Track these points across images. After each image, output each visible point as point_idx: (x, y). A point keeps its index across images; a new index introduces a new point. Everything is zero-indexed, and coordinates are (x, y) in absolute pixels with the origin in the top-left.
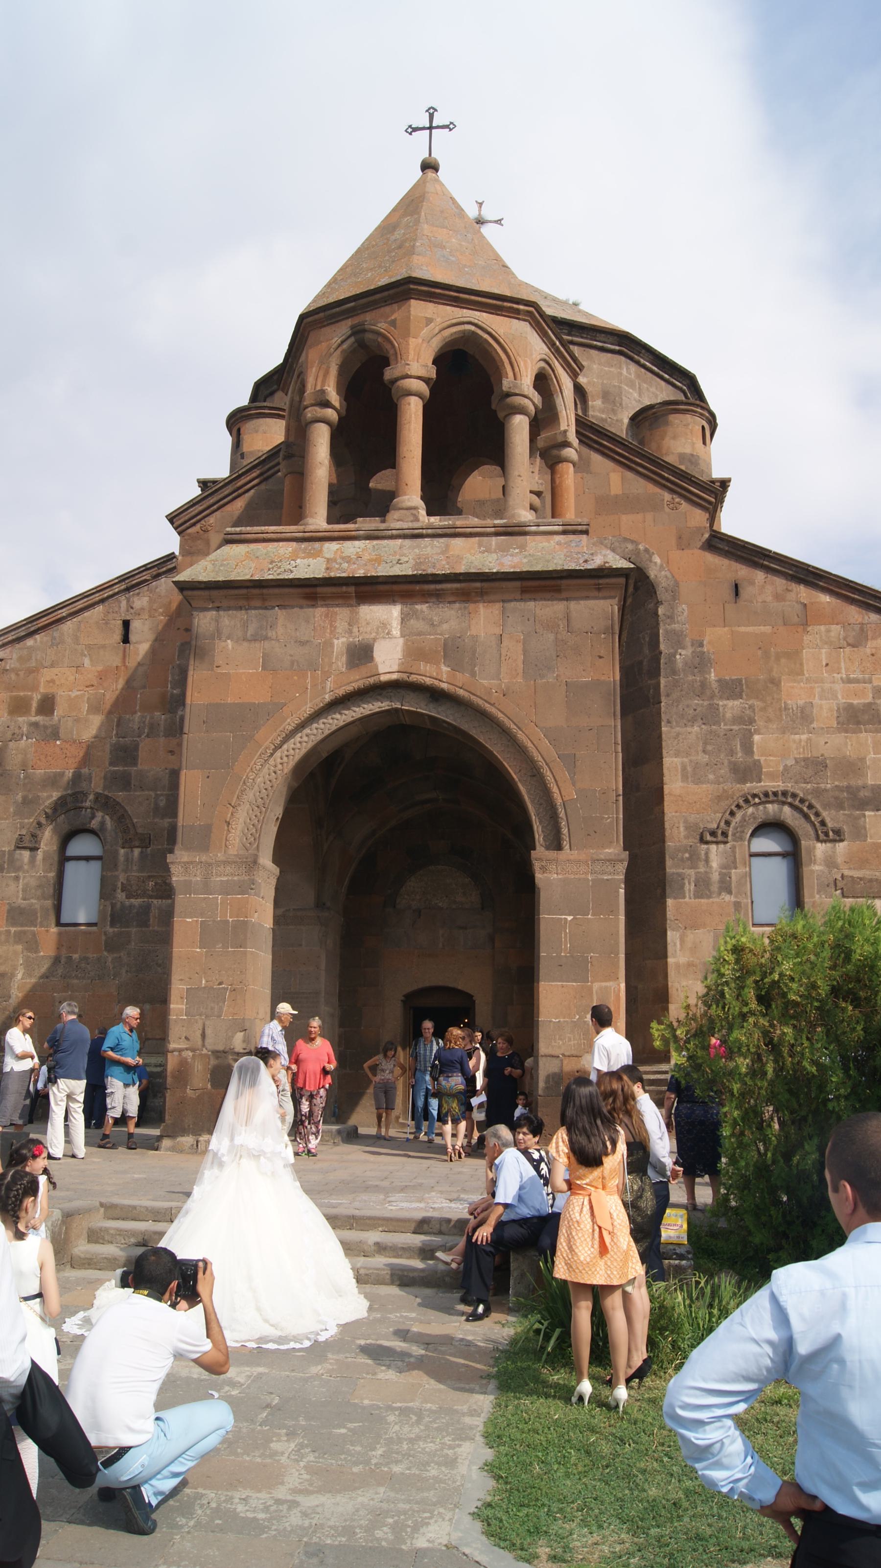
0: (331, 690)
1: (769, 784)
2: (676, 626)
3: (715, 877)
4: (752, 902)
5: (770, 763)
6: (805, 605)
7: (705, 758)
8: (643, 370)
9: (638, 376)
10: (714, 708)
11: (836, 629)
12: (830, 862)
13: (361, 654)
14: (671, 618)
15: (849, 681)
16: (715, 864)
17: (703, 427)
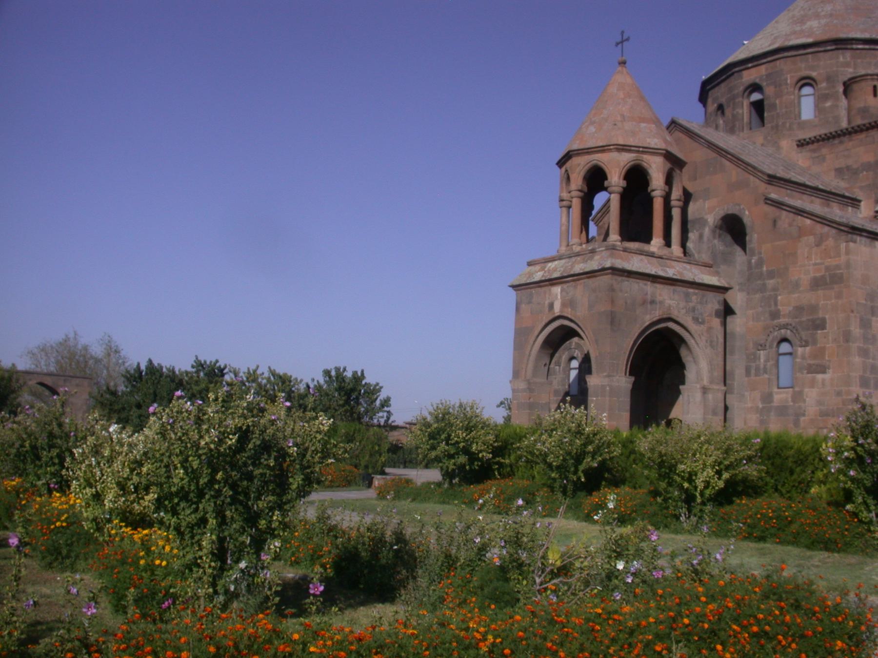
0: (546, 320)
1: (782, 321)
2: (752, 246)
3: (762, 366)
4: (778, 378)
5: (785, 309)
6: (800, 227)
7: (760, 309)
8: (858, 52)
10: (764, 285)
11: (811, 239)
12: (803, 358)
13: (551, 306)
14: (750, 241)
15: (815, 264)
16: (762, 361)
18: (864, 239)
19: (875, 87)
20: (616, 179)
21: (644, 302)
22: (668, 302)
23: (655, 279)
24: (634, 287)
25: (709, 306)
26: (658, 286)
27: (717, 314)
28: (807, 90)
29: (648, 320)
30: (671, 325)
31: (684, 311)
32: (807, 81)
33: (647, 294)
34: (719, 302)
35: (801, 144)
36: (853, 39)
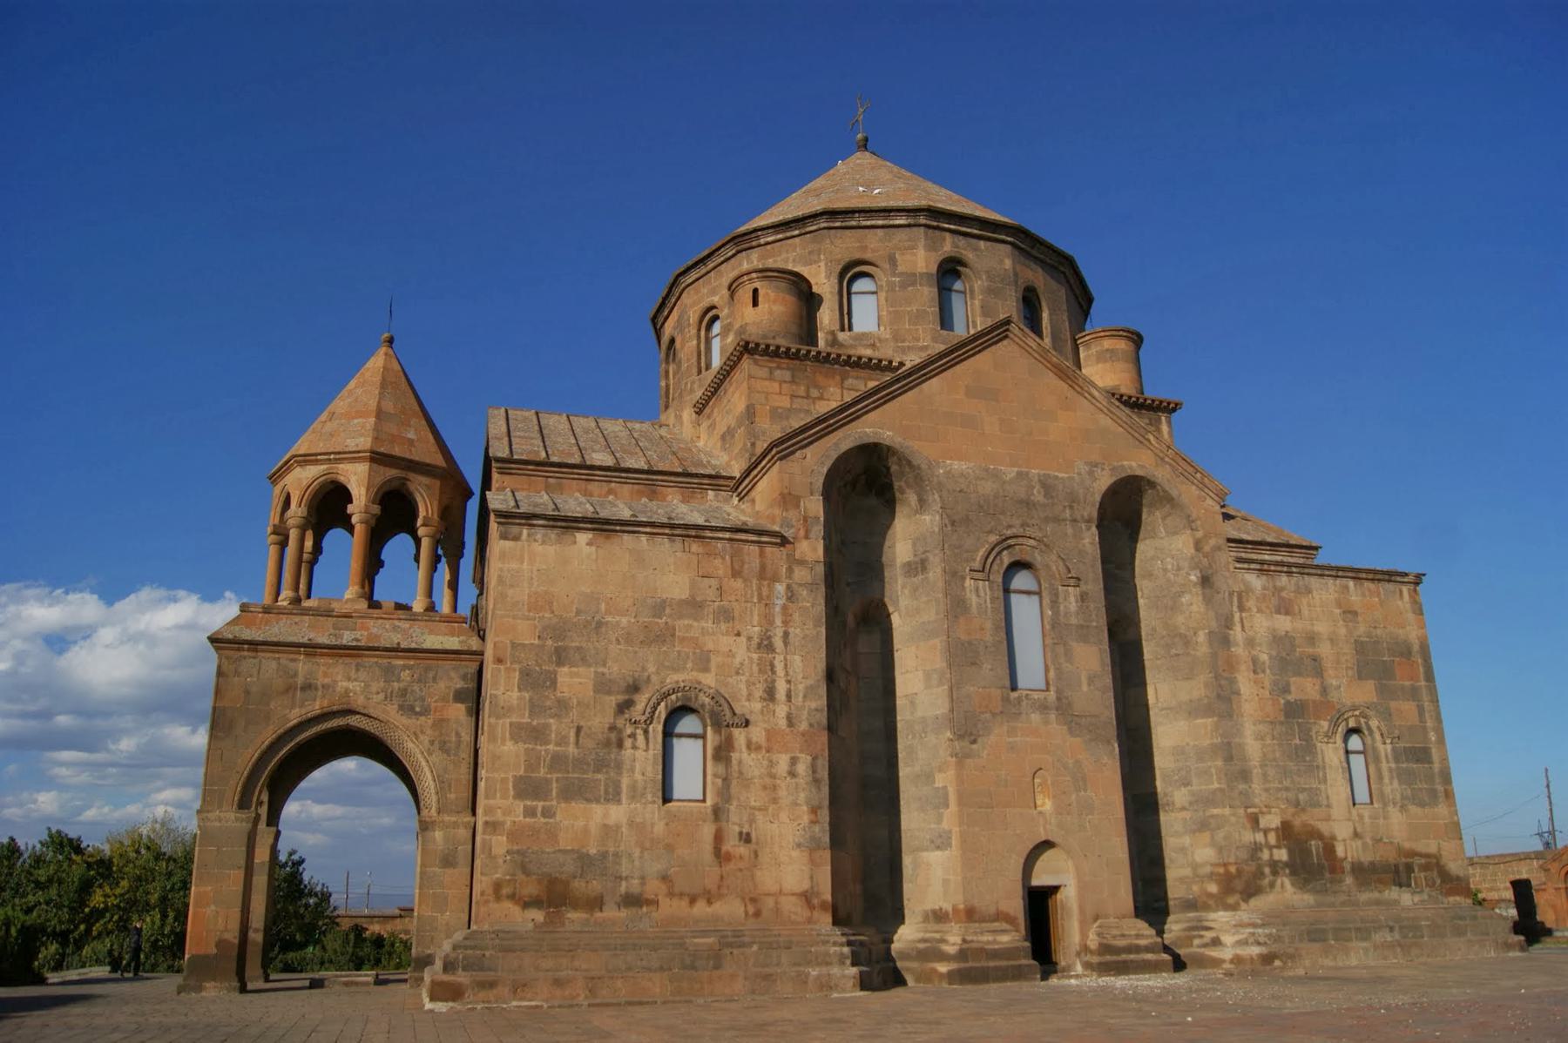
9: (761, 258)
17: (755, 291)
18: (540, 534)
19: (755, 291)
20: (297, 512)
21: (289, 689)
22: (343, 684)
23: (311, 649)
24: (269, 665)
25: (442, 685)
26: (322, 660)
27: (459, 696)
28: (717, 328)
29: (295, 716)
30: (354, 721)
31: (381, 696)
32: (709, 317)
33: (296, 675)
34: (464, 677)
35: (700, 408)
36: (755, 230)
